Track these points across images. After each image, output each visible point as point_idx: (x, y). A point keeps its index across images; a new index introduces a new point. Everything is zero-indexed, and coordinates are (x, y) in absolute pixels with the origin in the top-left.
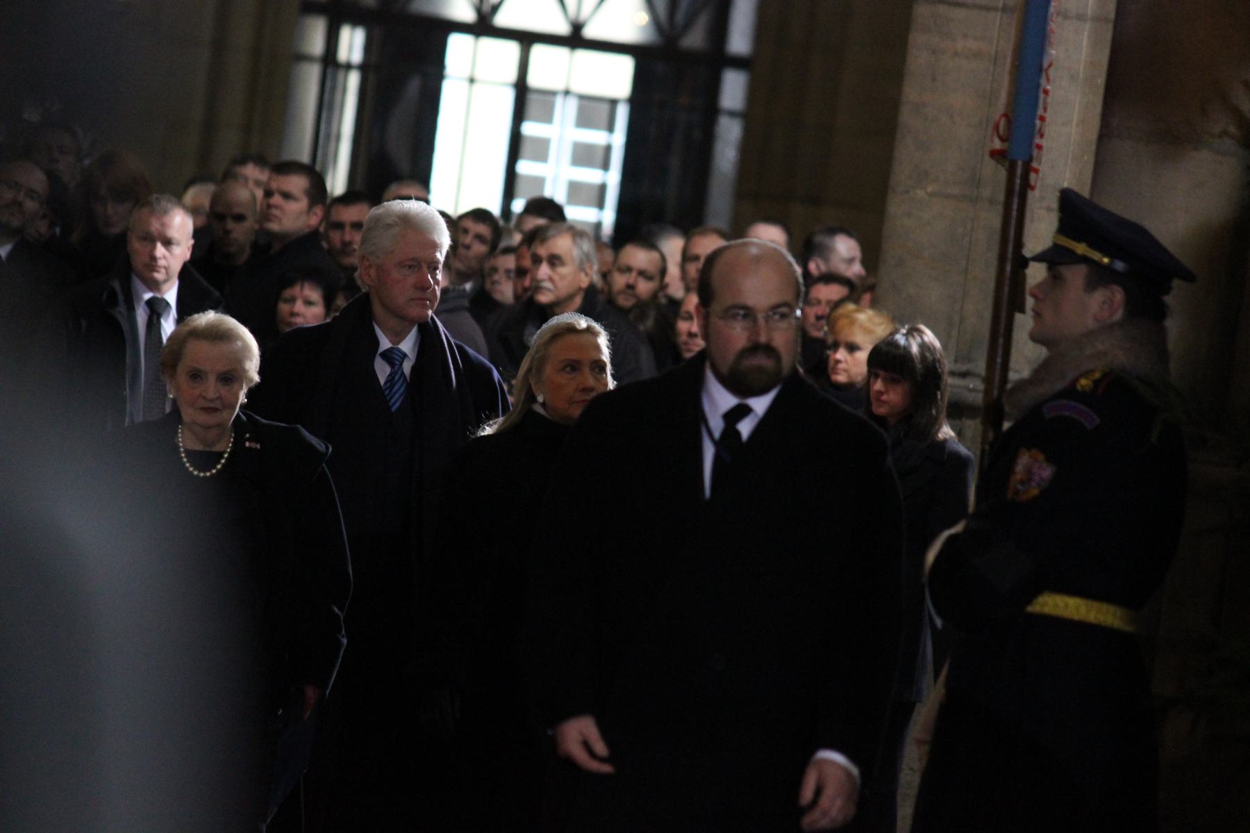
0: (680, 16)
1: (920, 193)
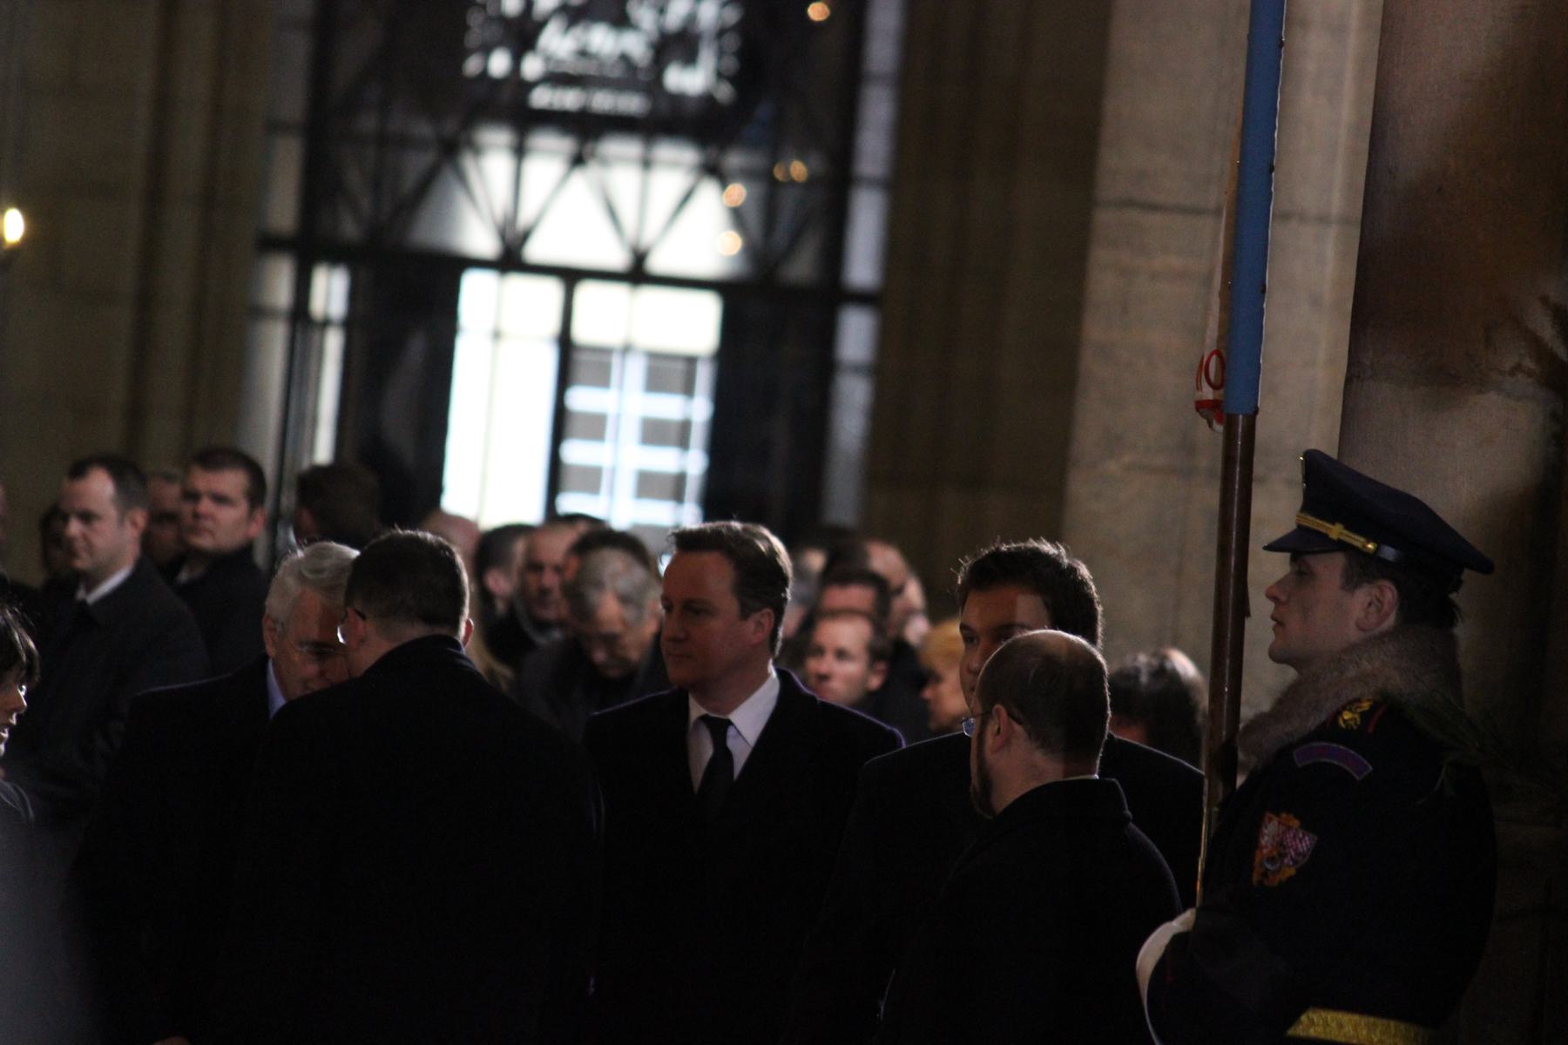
0: (781, 236)
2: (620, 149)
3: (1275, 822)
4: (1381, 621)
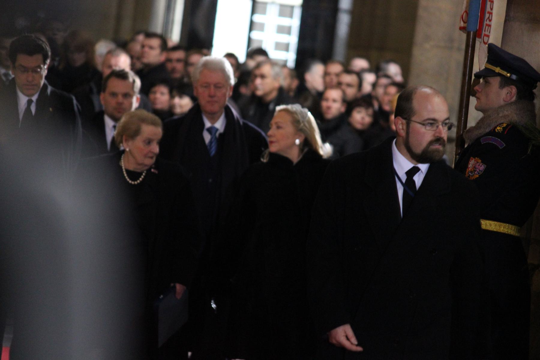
1: (427, 46)
3: (473, 160)
4: (511, 99)
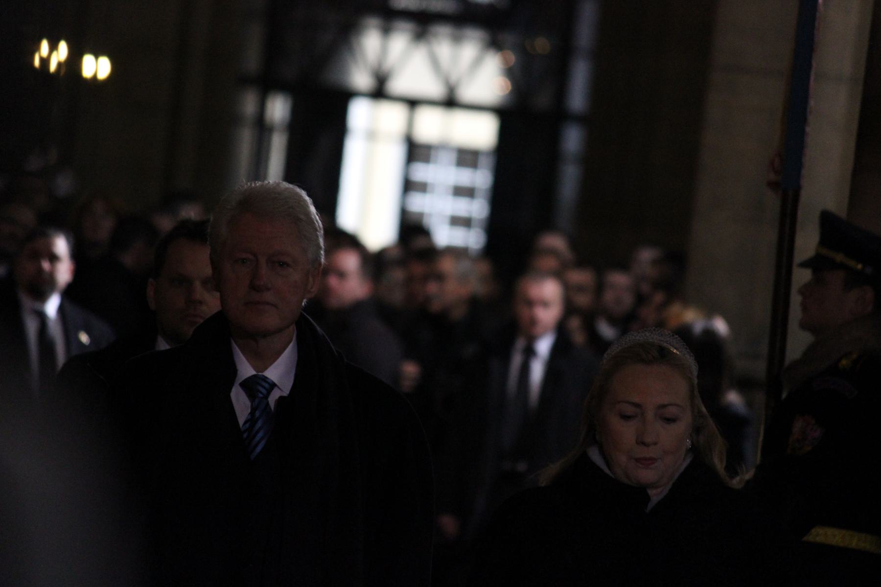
2: (443, 31)
